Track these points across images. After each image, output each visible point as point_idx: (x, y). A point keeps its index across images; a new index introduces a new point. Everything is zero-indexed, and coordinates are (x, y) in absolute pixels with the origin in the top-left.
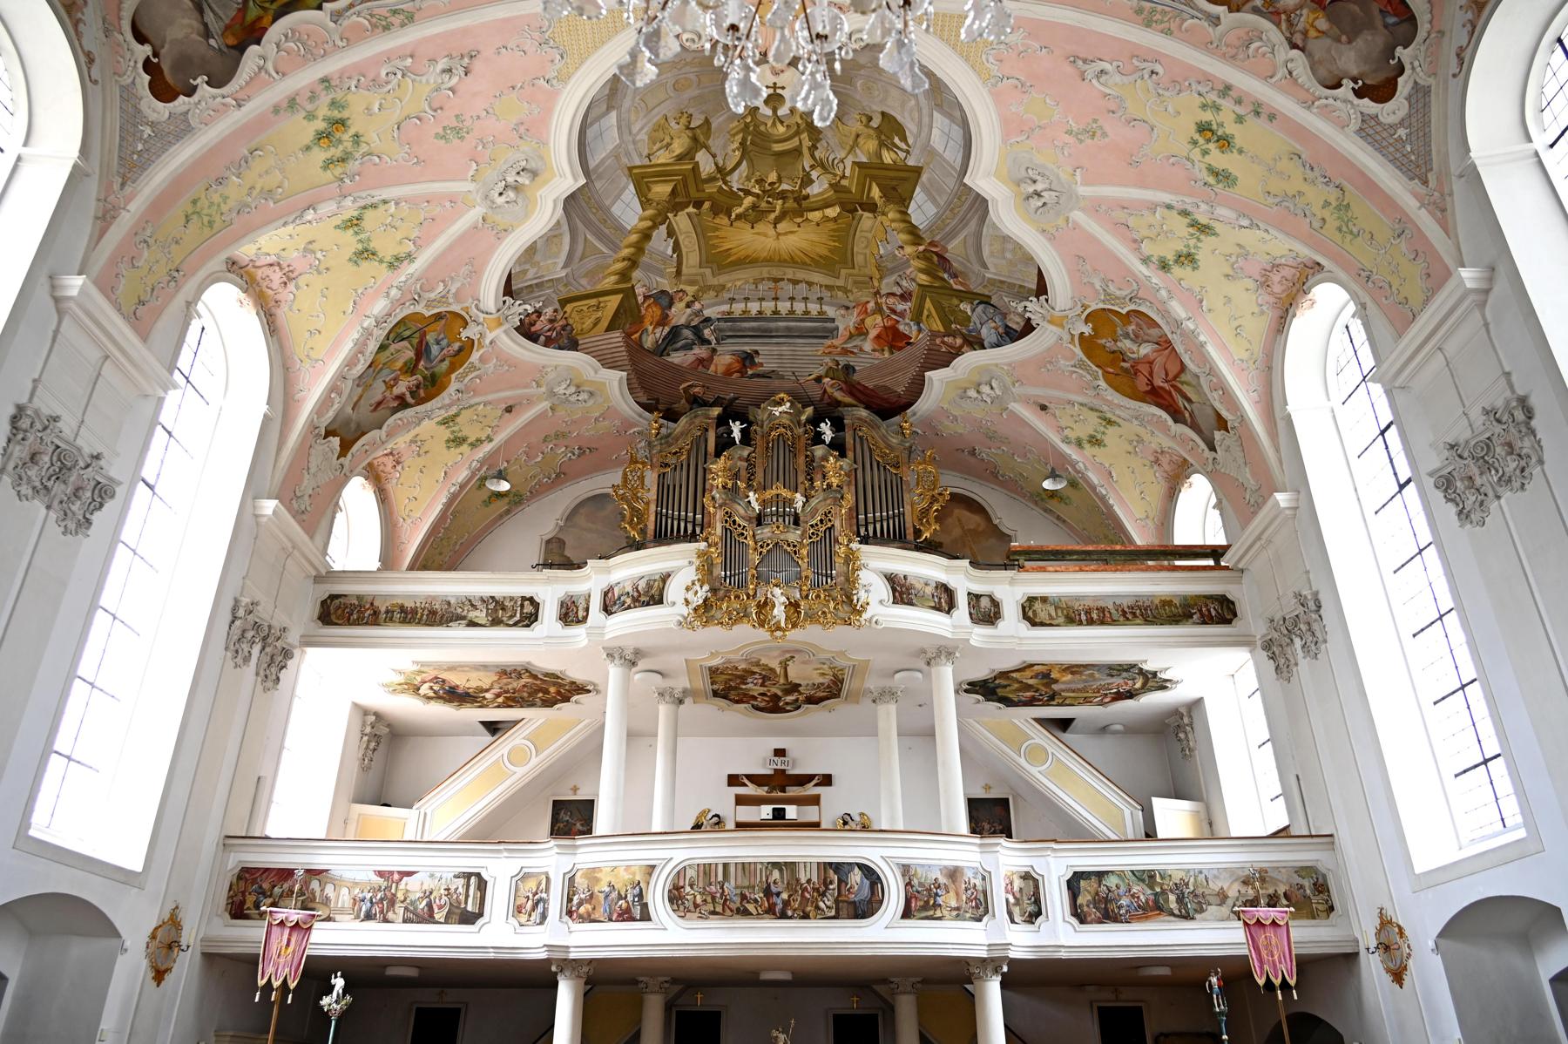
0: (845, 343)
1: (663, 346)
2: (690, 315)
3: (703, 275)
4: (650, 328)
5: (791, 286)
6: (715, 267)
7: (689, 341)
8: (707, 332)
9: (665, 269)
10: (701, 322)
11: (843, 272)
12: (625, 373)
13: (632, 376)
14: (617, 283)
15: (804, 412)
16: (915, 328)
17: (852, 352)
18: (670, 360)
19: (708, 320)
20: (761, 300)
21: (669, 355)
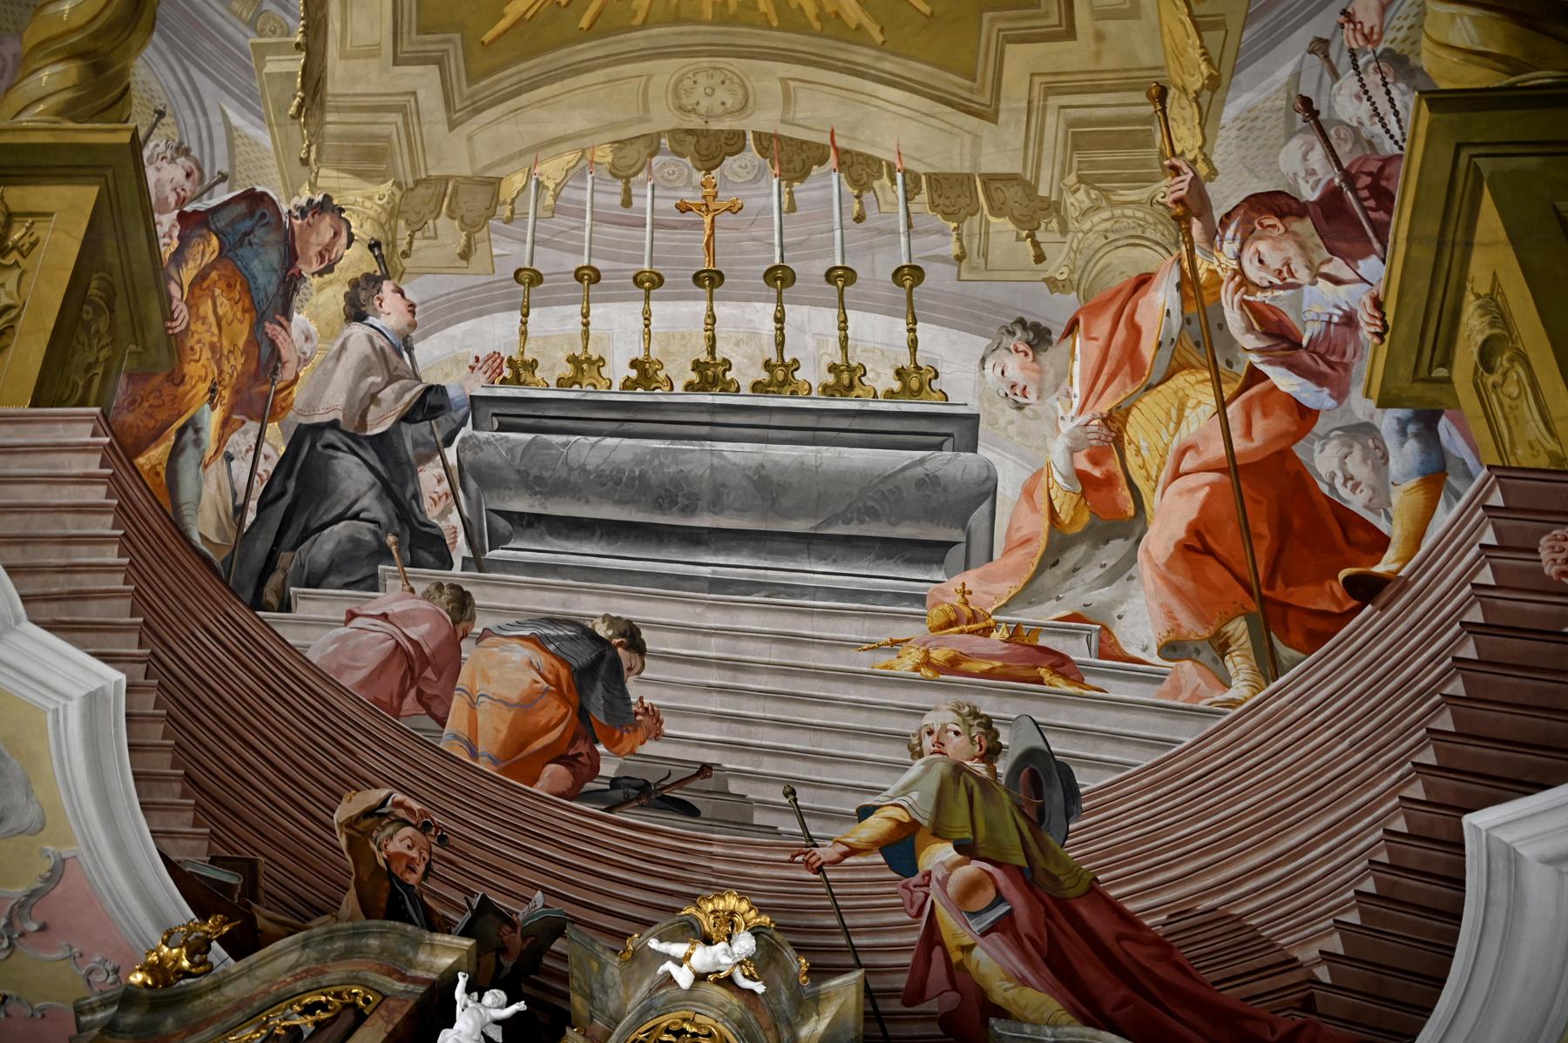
0: (1027, 594)
1: (261, 547)
2: (364, 370)
3: (406, 107)
4: (212, 420)
5: (771, 191)
6: (455, 62)
7: (364, 531)
8: (430, 479)
9: (261, 51)
10: (407, 417)
11: (1019, 58)
12: (114, 677)
13: (147, 703)
14: (69, 110)
15: (817, 1001)
16: (1404, 457)
17: (1062, 664)
18: (292, 636)
19: (431, 403)
20: (649, 283)
21: (286, 606)
